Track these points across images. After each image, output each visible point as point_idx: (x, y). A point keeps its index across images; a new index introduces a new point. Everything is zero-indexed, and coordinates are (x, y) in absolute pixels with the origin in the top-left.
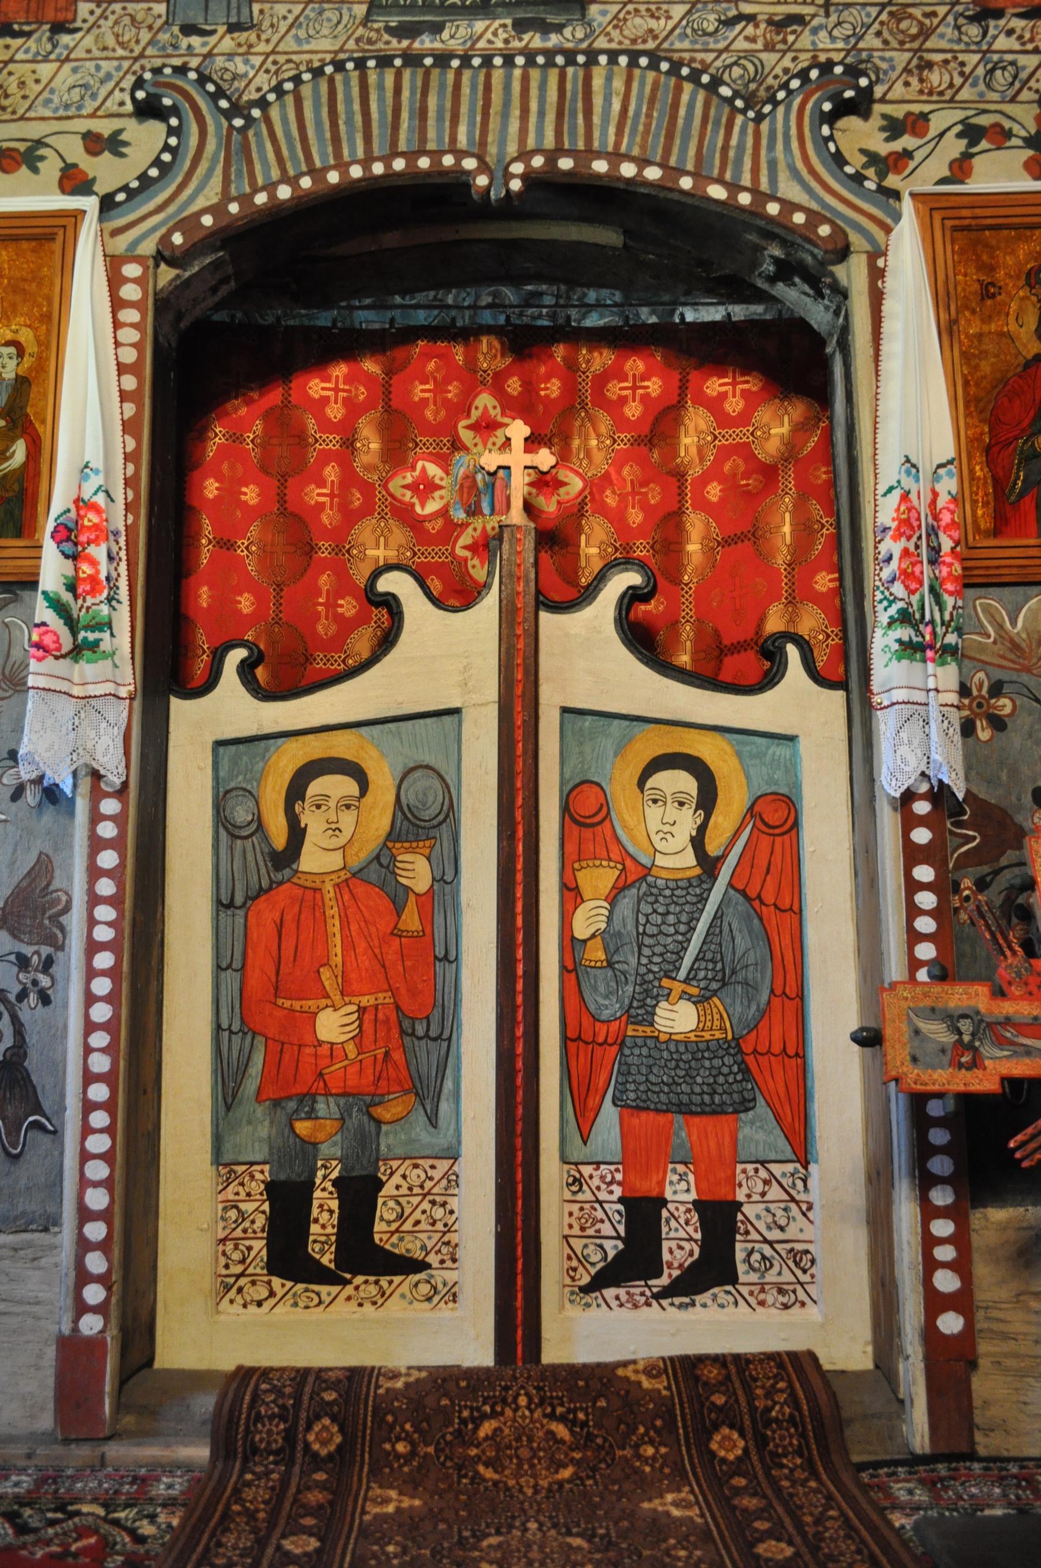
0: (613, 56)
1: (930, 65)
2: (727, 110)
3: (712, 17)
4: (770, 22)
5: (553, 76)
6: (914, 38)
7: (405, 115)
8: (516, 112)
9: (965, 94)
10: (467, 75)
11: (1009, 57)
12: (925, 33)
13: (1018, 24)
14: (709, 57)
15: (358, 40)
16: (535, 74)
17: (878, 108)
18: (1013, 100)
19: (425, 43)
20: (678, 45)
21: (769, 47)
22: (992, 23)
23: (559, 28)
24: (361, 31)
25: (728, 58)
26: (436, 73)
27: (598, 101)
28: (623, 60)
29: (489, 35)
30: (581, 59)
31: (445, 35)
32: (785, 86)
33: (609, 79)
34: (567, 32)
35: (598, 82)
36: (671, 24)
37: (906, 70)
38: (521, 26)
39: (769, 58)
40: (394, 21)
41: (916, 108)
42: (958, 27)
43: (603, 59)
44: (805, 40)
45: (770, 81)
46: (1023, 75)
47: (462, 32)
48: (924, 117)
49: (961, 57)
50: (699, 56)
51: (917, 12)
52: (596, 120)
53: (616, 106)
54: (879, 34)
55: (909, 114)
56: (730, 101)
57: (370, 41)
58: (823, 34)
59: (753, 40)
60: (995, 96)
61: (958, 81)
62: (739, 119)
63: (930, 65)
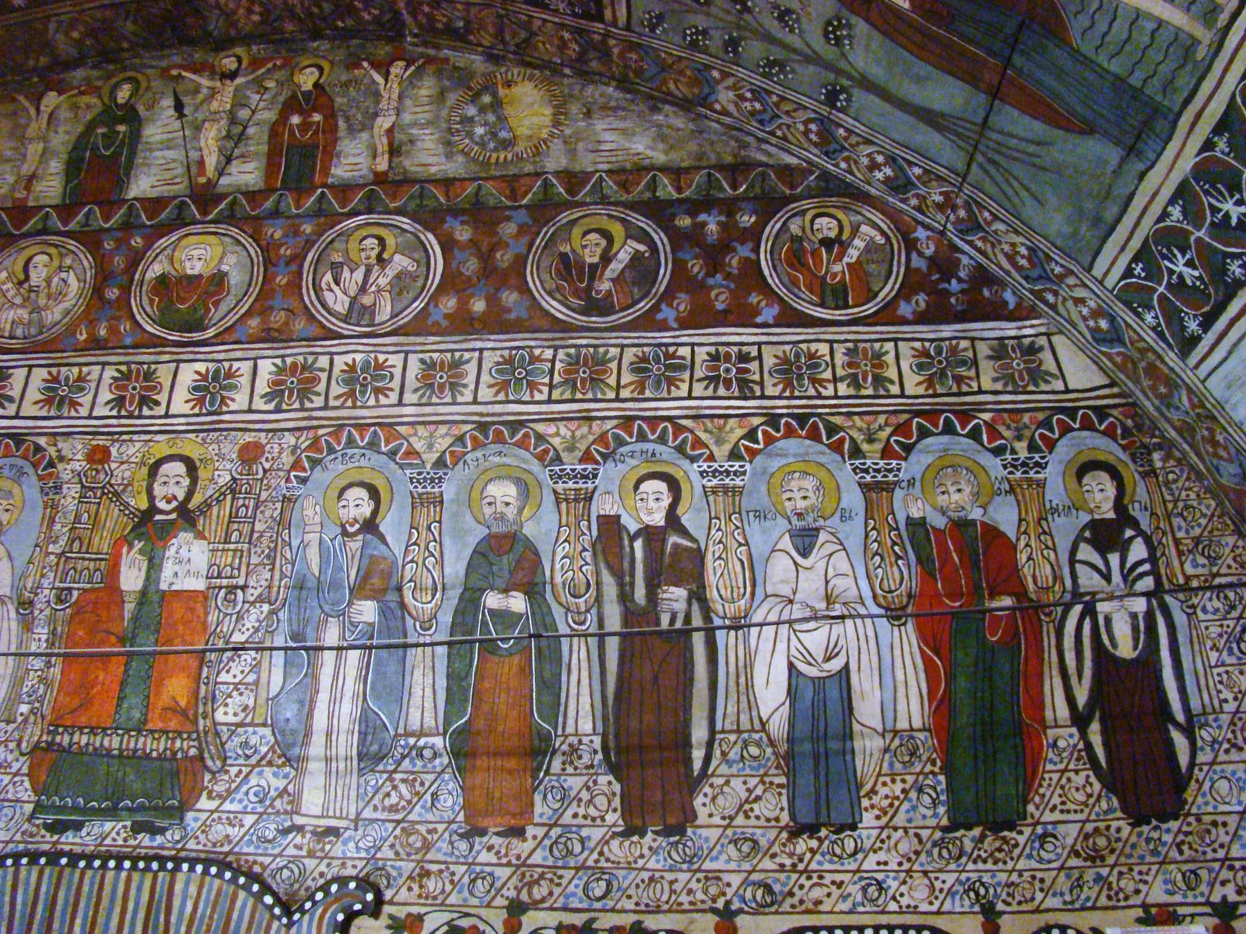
0: (193, 862)
1: (428, 874)
2: (267, 916)
3: (273, 826)
4: (314, 833)
5: (149, 877)
6: (418, 851)
7: (40, 908)
8: (118, 910)
9: (452, 899)
10: (89, 873)
11: (488, 869)
12: (427, 846)
13: (497, 841)
14: (267, 860)
15: (23, 833)
16: (136, 876)
17: (387, 909)
18: (488, 906)
19: (69, 840)
20: (245, 850)
21: (311, 854)
22: (477, 839)
23: (162, 831)
24: (26, 826)
25: (280, 862)
26: (68, 871)
27: (176, 903)
28: (199, 868)
29: (113, 834)
30: (170, 865)
31: (84, 832)
32: (311, 898)
33: (187, 884)
34: (169, 834)
35: (179, 887)
36: (243, 830)
37: (410, 877)
38: (137, 828)
39: (310, 863)
40: (50, 818)
41: (415, 910)
42: (451, 843)
43: (185, 866)
44: (338, 850)
45: (309, 882)
46: (498, 884)
47: (96, 830)
48: (420, 918)
49: (452, 868)
50: (260, 859)
51: (422, 829)
52: (173, 919)
53: (189, 908)
54: (392, 846)
55: (409, 915)
56: (270, 908)
57: (32, 835)
58: (351, 845)
59: (299, 847)
60: (475, 901)
61: (448, 887)
62: (276, 924)
63: (428, 874)
